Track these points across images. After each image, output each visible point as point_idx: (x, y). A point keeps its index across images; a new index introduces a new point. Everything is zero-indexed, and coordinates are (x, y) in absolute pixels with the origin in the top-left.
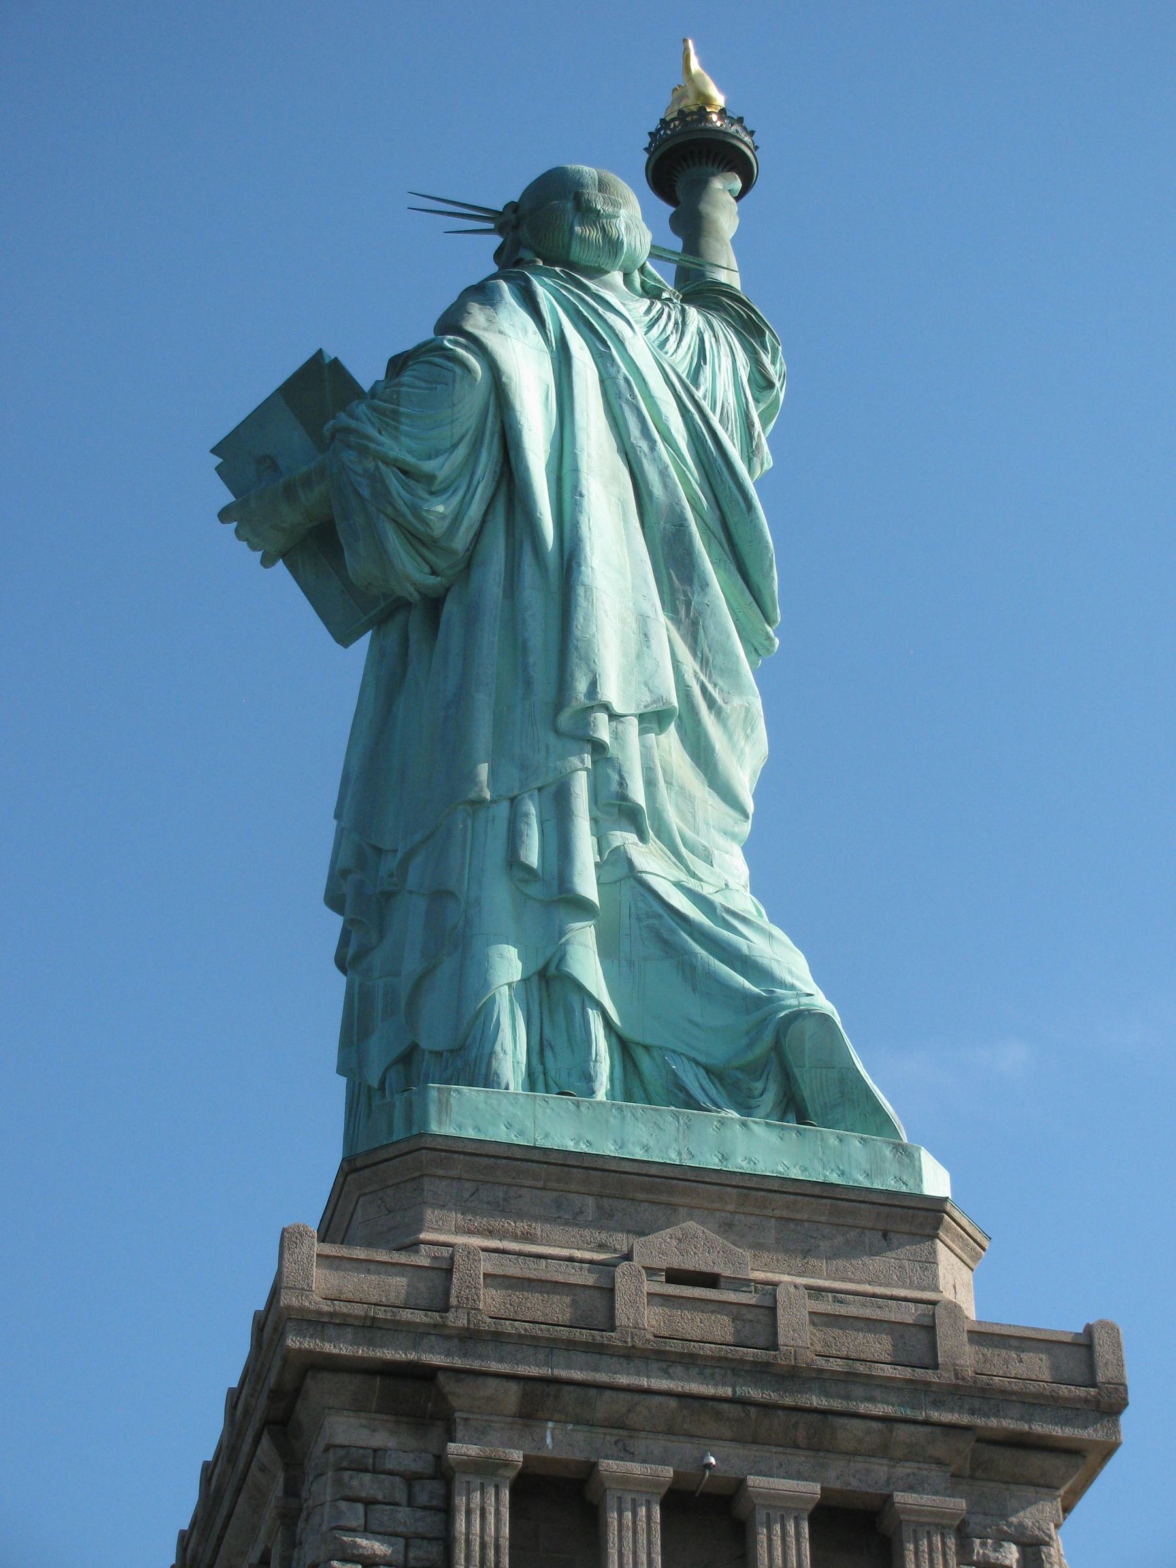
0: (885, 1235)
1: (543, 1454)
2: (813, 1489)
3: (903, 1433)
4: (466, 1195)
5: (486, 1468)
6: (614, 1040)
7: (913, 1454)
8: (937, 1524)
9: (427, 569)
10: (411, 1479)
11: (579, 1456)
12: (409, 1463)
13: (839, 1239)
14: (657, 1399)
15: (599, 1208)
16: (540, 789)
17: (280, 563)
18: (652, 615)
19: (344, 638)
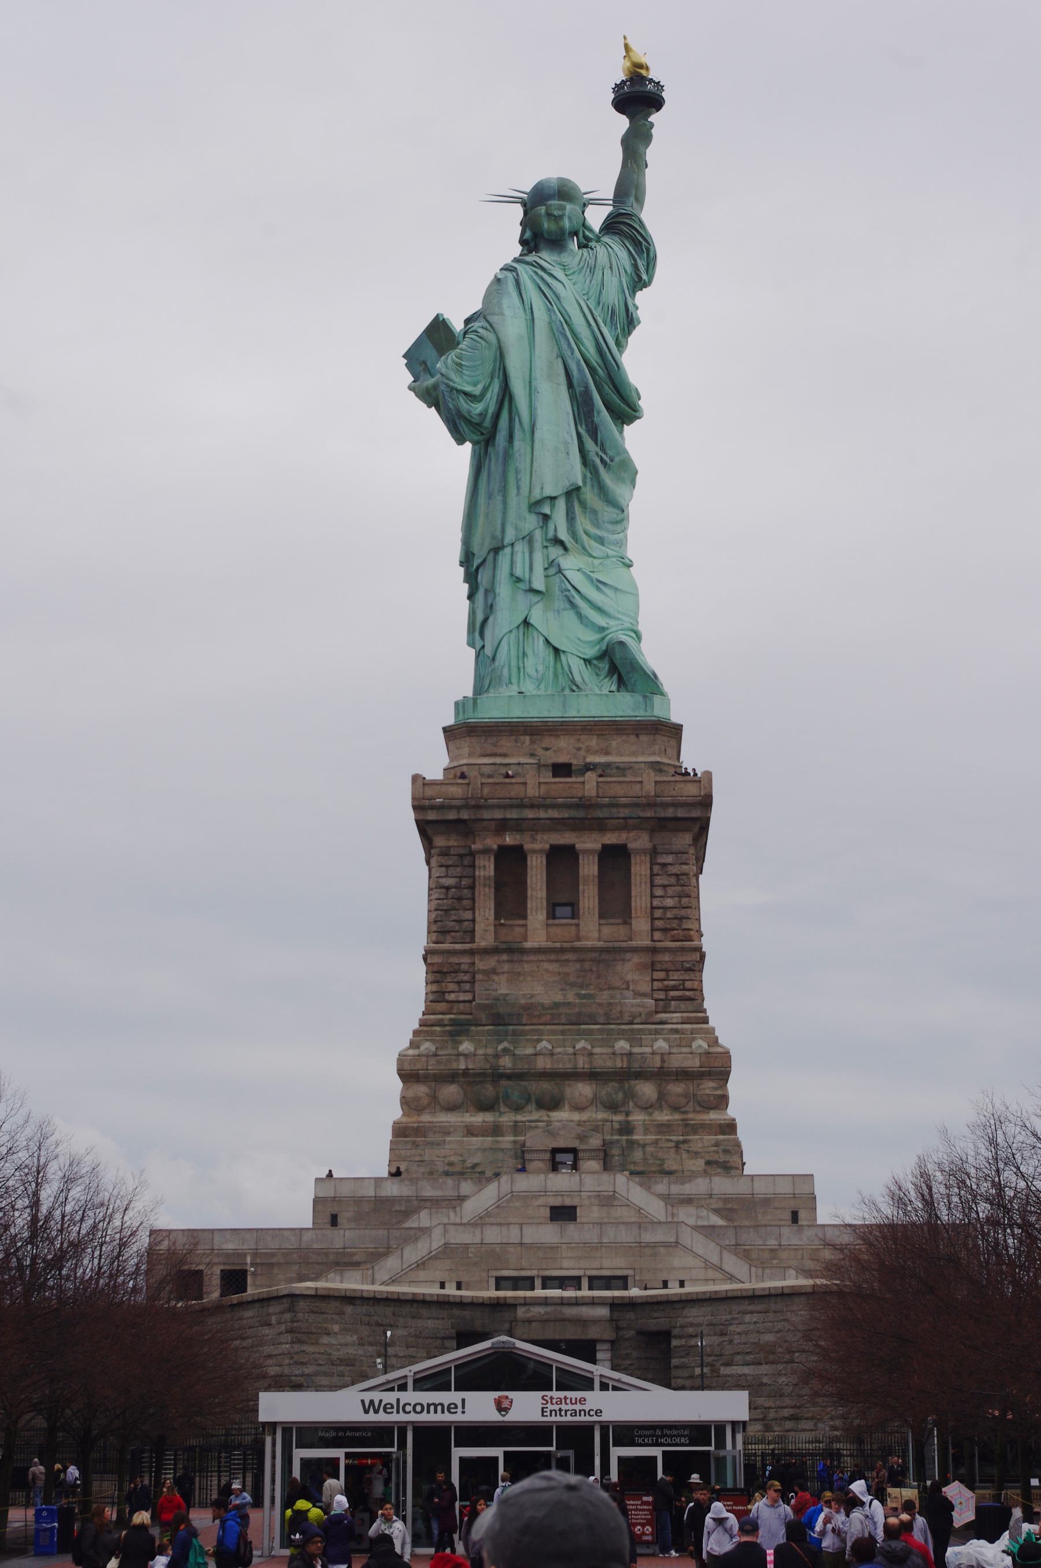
0: (637, 736)
1: (505, 843)
2: (598, 846)
3: (630, 822)
4: (482, 741)
5: (486, 851)
6: (551, 649)
7: (635, 828)
8: (643, 851)
9: (479, 433)
10: (461, 856)
11: (517, 843)
12: (462, 851)
13: (620, 740)
14: (543, 821)
15: (531, 740)
16: (523, 538)
17: (433, 408)
18: (570, 441)
19: (460, 440)
